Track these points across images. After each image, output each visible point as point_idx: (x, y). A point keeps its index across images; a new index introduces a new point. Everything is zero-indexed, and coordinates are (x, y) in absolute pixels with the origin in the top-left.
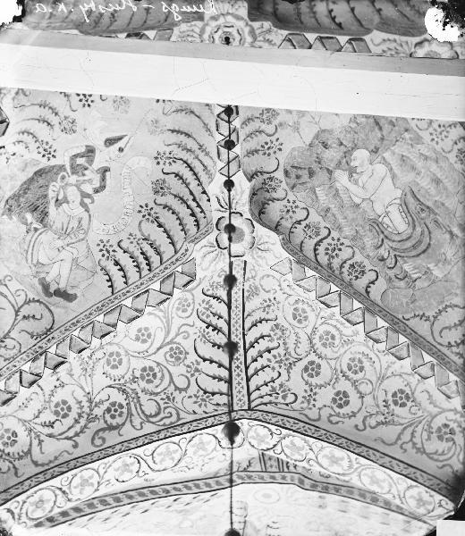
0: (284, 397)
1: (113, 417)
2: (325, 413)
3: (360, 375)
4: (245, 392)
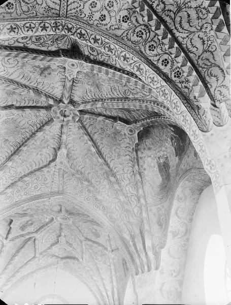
0: (81, 15)
1: (9, 8)
2: (96, 22)
3: (112, 8)
4: (65, 10)
